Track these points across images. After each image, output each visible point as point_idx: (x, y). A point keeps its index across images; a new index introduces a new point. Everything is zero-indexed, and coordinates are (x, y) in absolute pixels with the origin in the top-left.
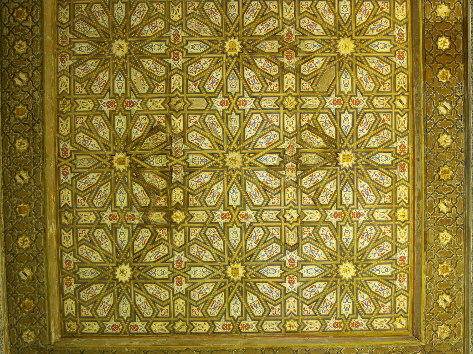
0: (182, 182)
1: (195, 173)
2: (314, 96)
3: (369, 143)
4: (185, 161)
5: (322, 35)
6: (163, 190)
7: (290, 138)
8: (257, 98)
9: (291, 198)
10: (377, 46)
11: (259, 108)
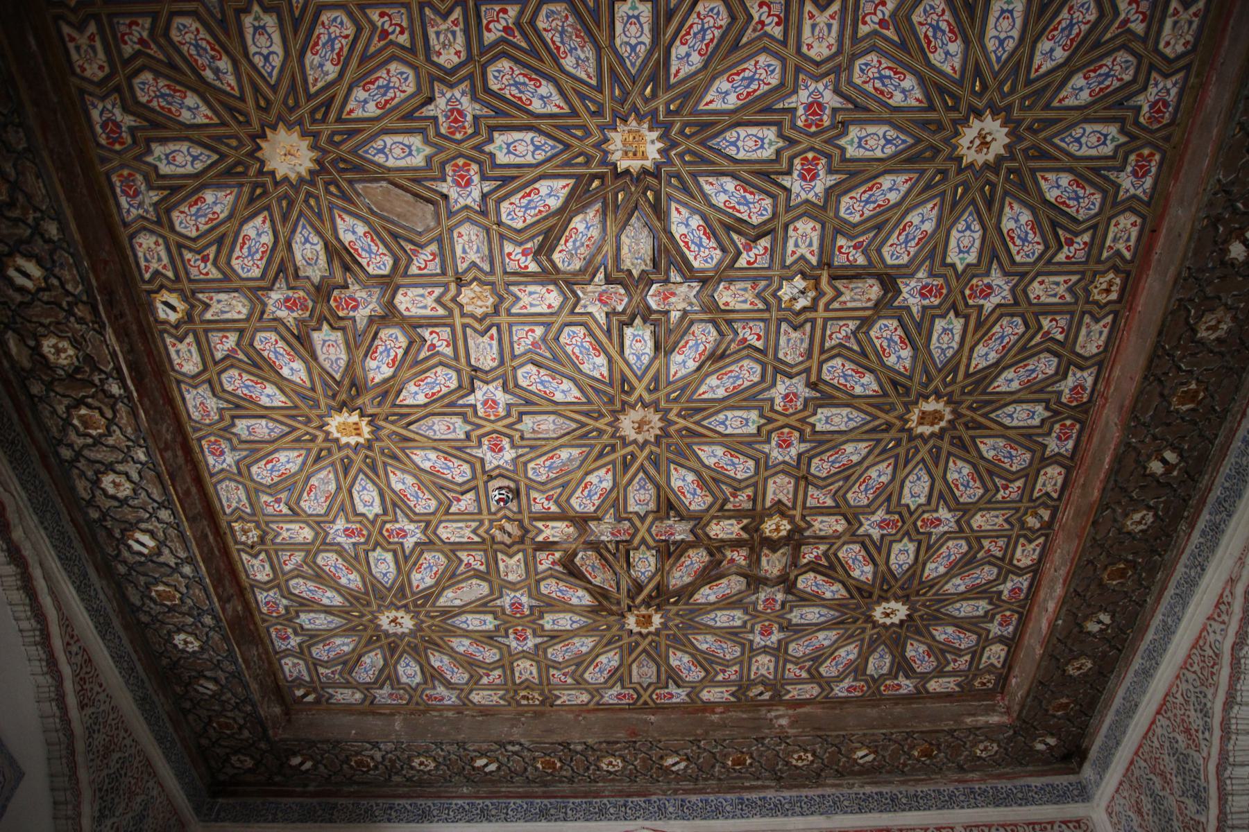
0: (692, 523)
1: (672, 497)
2: (451, 238)
3: (583, 76)
4: (642, 519)
5: (272, 221)
6: (711, 554)
7: (578, 299)
8: (473, 376)
9: (749, 296)
10: (266, 58)
11: (500, 371)
